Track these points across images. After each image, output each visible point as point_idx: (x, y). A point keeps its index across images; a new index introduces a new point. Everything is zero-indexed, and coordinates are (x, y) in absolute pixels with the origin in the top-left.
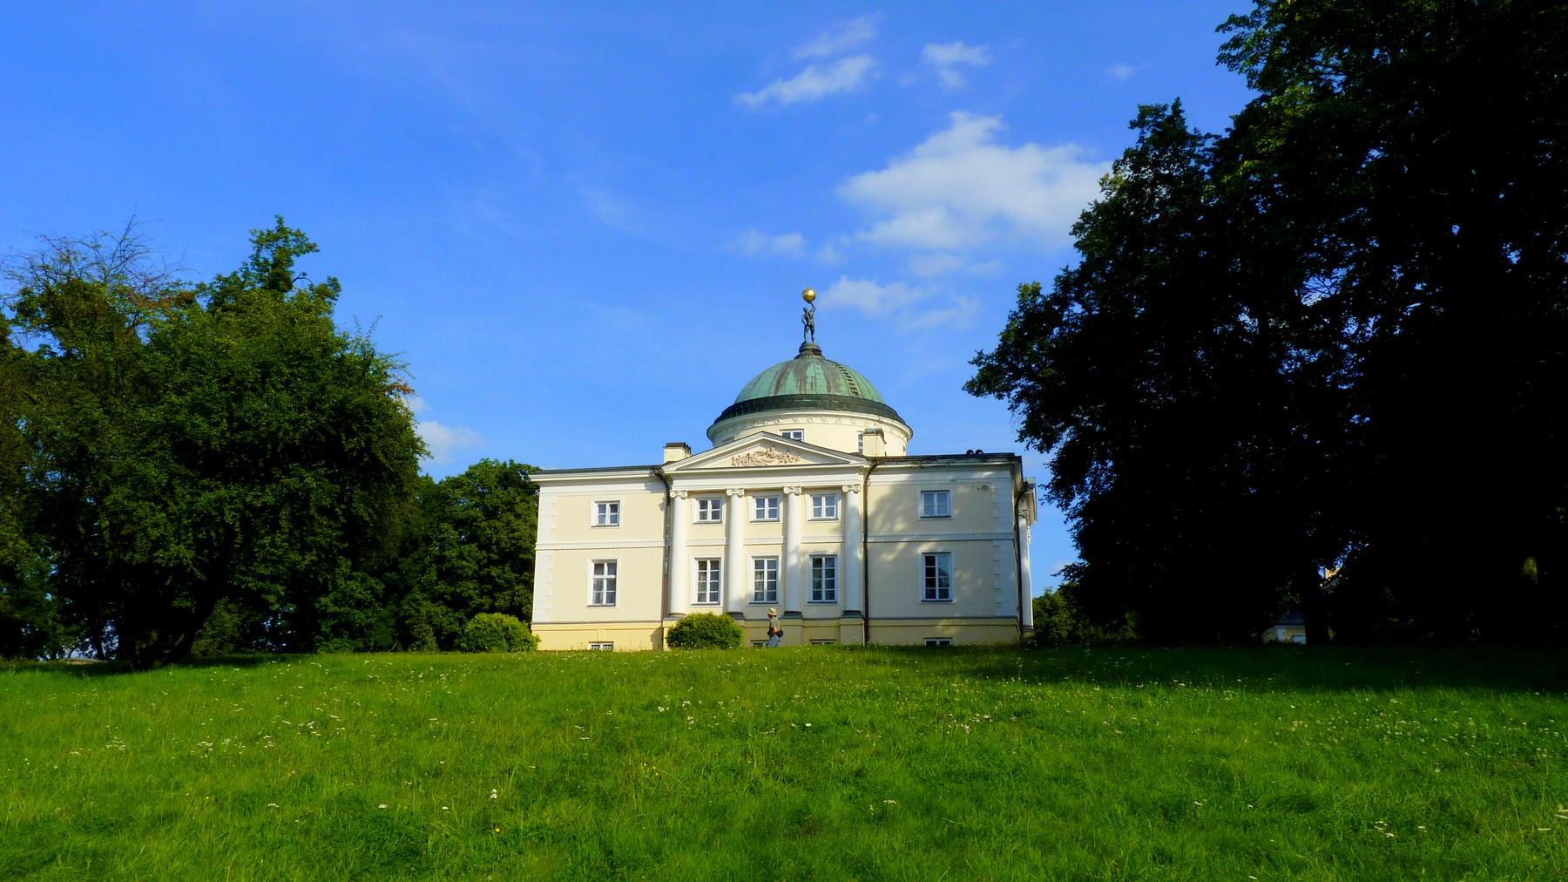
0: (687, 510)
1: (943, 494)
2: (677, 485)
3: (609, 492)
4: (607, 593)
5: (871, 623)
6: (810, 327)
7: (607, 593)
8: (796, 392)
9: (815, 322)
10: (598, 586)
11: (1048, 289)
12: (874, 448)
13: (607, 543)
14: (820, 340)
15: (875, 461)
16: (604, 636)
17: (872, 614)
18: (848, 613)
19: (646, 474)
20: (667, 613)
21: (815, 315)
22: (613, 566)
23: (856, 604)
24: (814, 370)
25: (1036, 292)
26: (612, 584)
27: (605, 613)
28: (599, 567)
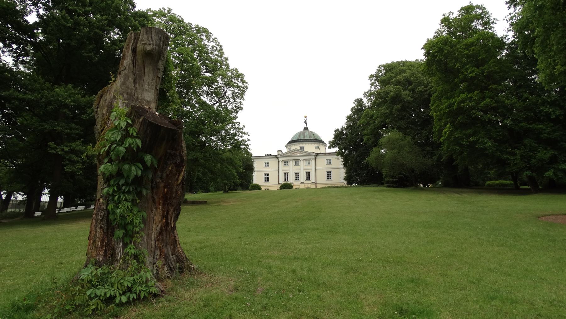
0: (281, 164)
1: (330, 160)
2: (280, 159)
3: (267, 160)
4: (267, 180)
6: (306, 123)
10: (265, 178)
11: (340, 130)
12: (318, 151)
13: (267, 170)
14: (308, 126)
15: (318, 154)
16: (267, 188)
18: (313, 182)
20: (279, 184)
22: (268, 175)
23: (314, 181)
24: (306, 133)
25: (338, 130)
26: (268, 178)
27: (267, 183)
28: (265, 175)
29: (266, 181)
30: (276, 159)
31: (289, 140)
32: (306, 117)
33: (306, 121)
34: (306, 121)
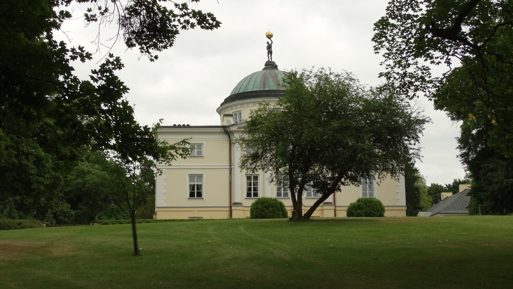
2: (237, 136)
4: (196, 192)
5: (337, 209)
6: (270, 52)
7: (196, 192)
8: (275, 89)
9: (273, 49)
10: (192, 187)
14: (275, 59)
16: (196, 214)
17: (337, 204)
19: (219, 130)
21: (273, 45)
26: (199, 187)
27: (196, 202)
29: (192, 195)
30: (225, 137)
31: (228, 95)
32: (269, 37)
33: (269, 47)
34: (269, 47)
